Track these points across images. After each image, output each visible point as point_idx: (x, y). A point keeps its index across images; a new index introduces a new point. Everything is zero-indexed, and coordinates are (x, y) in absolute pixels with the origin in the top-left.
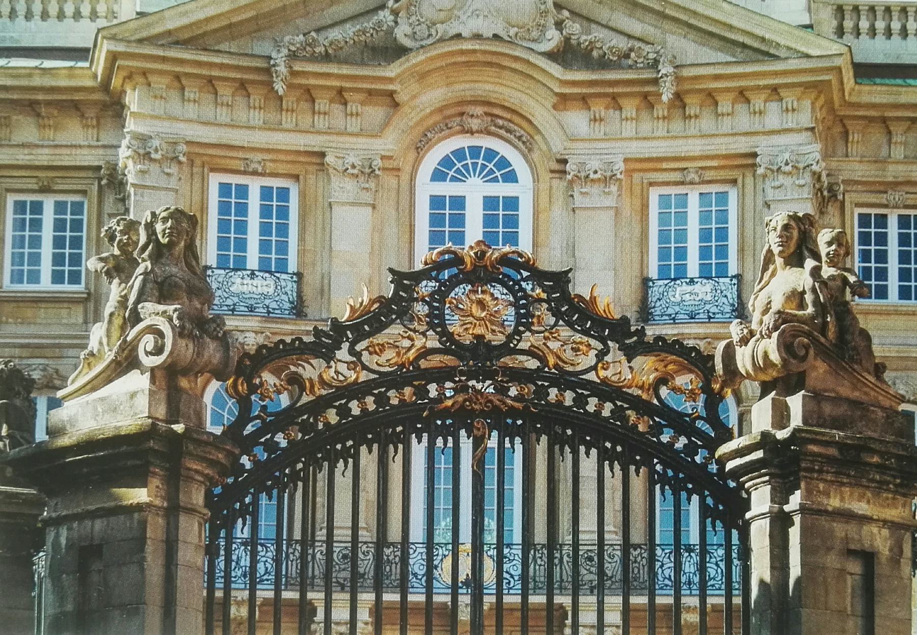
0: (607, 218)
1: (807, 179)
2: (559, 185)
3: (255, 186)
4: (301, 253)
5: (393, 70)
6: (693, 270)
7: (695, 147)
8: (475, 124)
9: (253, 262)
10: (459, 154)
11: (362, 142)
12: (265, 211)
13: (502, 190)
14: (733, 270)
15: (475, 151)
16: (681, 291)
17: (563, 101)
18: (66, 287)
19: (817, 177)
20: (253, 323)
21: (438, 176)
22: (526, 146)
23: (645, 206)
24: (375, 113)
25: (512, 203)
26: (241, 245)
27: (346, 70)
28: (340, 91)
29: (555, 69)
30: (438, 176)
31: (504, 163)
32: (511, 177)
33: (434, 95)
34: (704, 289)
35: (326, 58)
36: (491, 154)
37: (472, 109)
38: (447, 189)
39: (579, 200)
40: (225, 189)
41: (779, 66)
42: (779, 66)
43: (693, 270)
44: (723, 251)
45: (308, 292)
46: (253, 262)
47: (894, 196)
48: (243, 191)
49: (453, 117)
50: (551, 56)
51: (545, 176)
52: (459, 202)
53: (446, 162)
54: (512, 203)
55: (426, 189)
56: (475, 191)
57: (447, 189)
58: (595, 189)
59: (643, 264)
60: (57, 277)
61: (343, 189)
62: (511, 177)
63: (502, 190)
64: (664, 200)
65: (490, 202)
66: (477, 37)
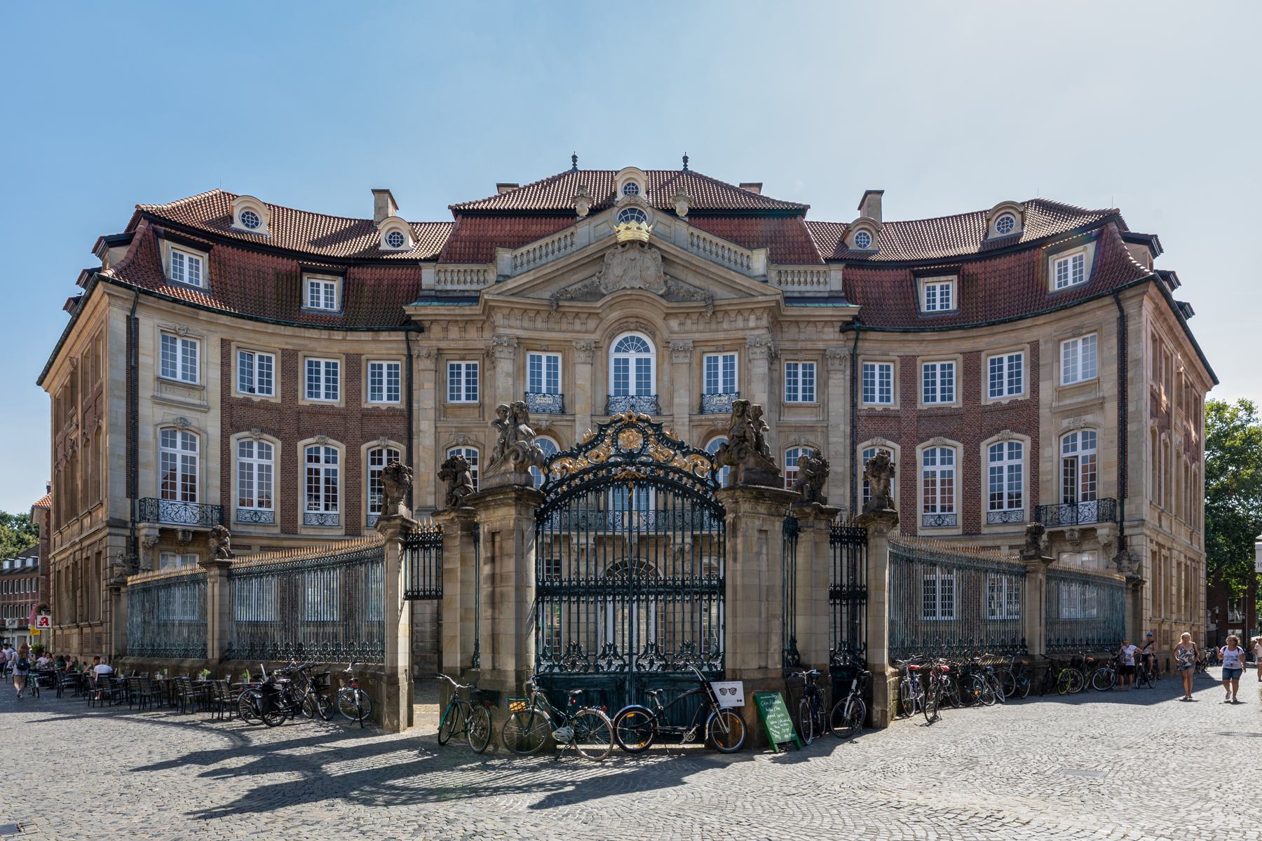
0: (685, 367)
1: (765, 349)
2: (666, 353)
3: (544, 356)
4: (563, 385)
5: (599, 304)
6: (720, 391)
7: (721, 336)
8: (632, 326)
9: (544, 390)
10: (626, 339)
11: (587, 336)
12: (549, 367)
13: (643, 356)
14: (736, 390)
15: (632, 338)
16: (716, 399)
17: (667, 316)
18: (471, 402)
19: (769, 348)
20: (545, 417)
21: (618, 350)
22: (653, 335)
23: (701, 361)
24: (592, 324)
25: (648, 361)
26: (540, 382)
27: (580, 304)
28: (577, 313)
29: (664, 302)
30: (618, 350)
31: (644, 343)
32: (647, 350)
33: (615, 315)
34: (725, 399)
35: (572, 299)
36: (639, 339)
37: (630, 320)
38: (621, 356)
39: (675, 360)
40: (532, 357)
41: (755, 299)
42: (755, 299)
43: (720, 391)
44: (732, 382)
45: (566, 401)
46: (544, 390)
47: (801, 356)
48: (540, 358)
49: (622, 326)
50: (661, 296)
51: (661, 349)
52: (626, 361)
53: (620, 343)
54: (648, 361)
55: (614, 355)
56: (632, 356)
57: (621, 356)
58: (682, 355)
59: (701, 388)
60: (468, 397)
61: (581, 356)
62: (647, 350)
63: (643, 356)
64: (709, 359)
65: (639, 361)
66: (632, 288)
